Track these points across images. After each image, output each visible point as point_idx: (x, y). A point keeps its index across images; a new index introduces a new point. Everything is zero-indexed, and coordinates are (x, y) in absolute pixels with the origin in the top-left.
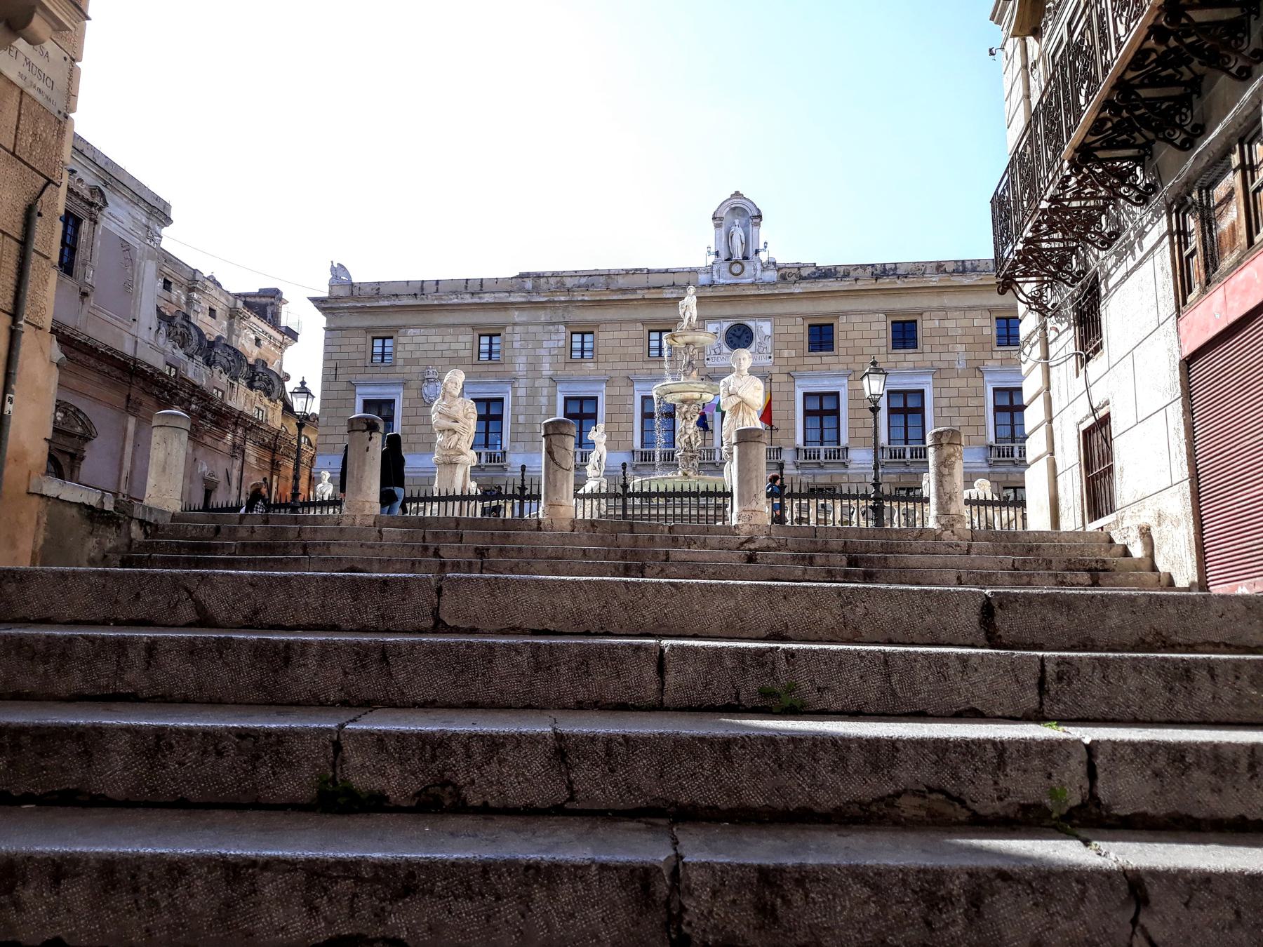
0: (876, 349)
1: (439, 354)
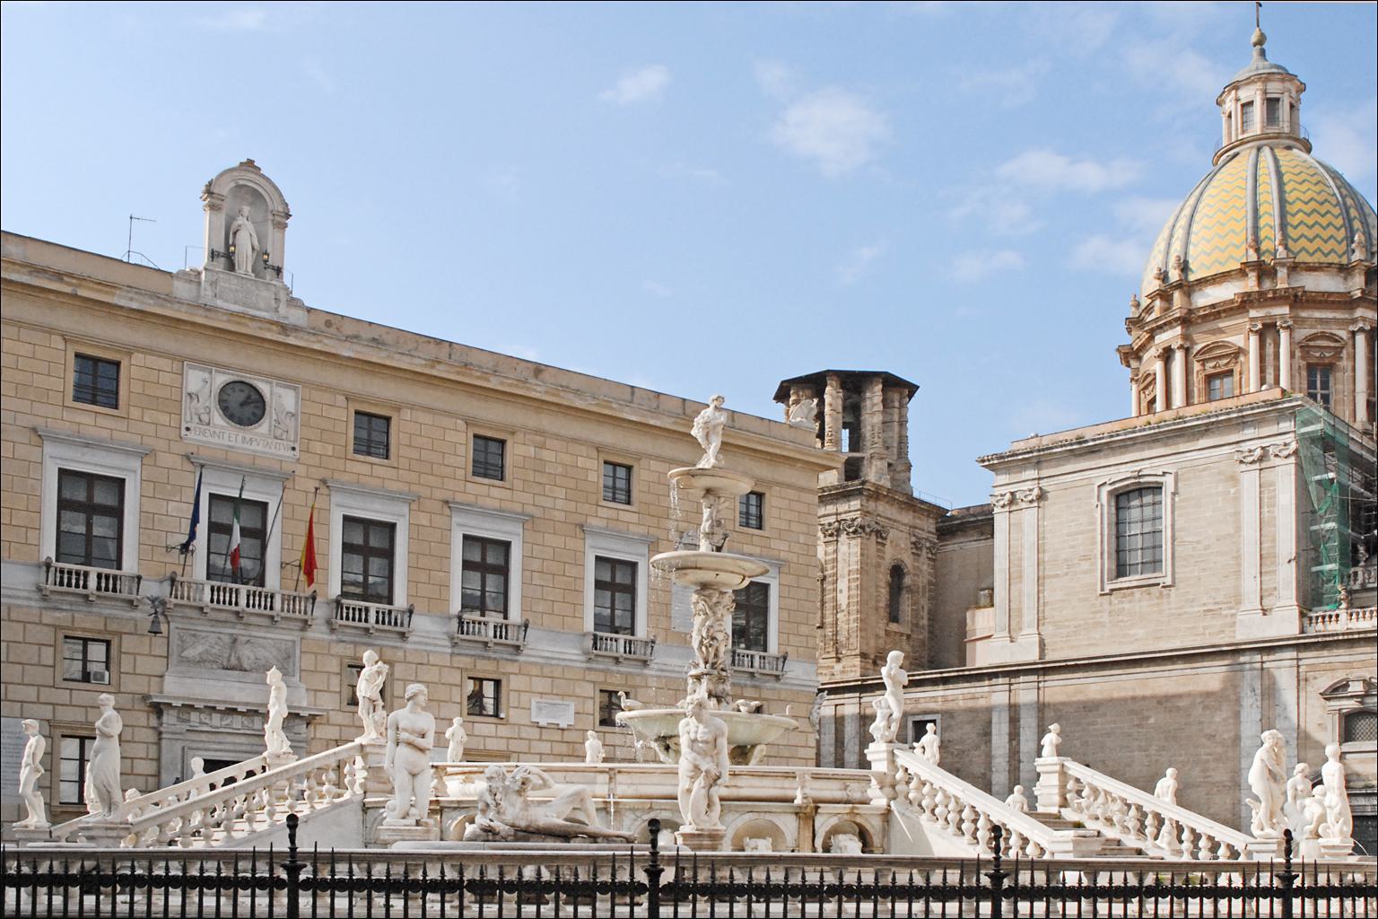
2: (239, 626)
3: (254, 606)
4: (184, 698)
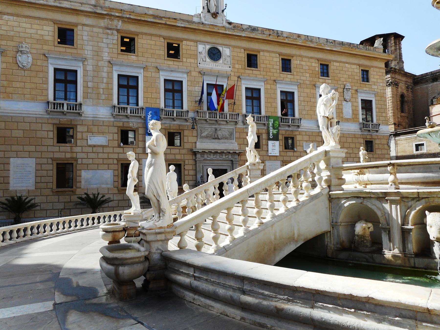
0: (276, 70)
1: (29, 36)
2: (217, 125)
3: (221, 118)
4: (203, 149)
